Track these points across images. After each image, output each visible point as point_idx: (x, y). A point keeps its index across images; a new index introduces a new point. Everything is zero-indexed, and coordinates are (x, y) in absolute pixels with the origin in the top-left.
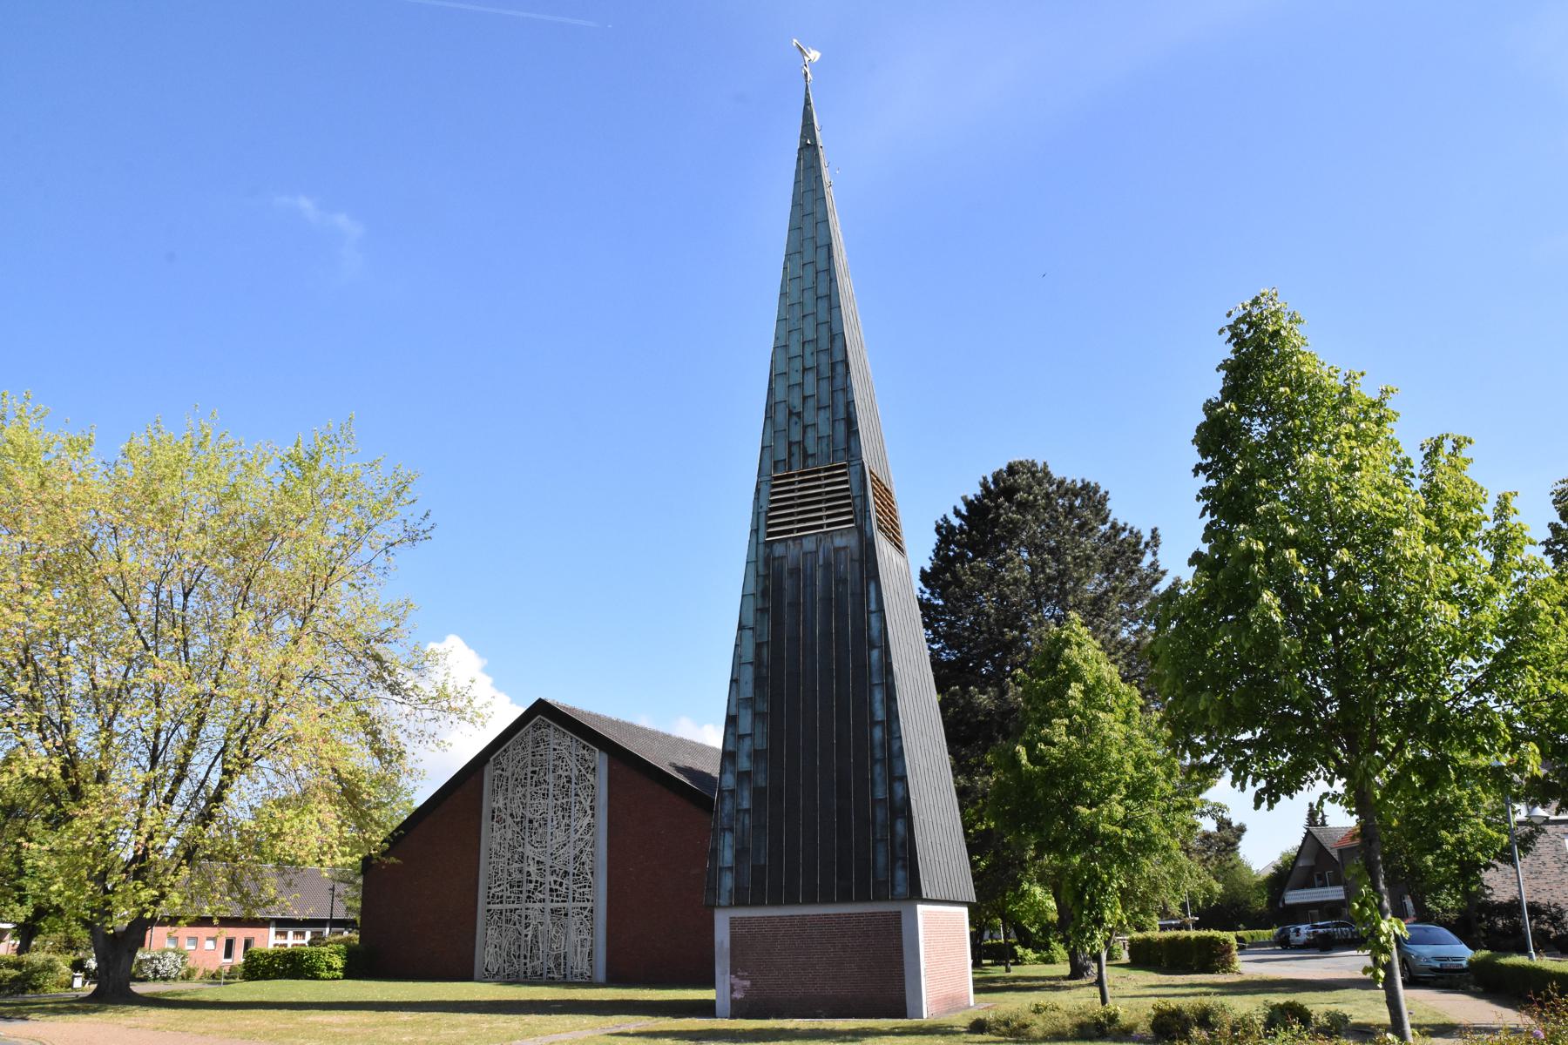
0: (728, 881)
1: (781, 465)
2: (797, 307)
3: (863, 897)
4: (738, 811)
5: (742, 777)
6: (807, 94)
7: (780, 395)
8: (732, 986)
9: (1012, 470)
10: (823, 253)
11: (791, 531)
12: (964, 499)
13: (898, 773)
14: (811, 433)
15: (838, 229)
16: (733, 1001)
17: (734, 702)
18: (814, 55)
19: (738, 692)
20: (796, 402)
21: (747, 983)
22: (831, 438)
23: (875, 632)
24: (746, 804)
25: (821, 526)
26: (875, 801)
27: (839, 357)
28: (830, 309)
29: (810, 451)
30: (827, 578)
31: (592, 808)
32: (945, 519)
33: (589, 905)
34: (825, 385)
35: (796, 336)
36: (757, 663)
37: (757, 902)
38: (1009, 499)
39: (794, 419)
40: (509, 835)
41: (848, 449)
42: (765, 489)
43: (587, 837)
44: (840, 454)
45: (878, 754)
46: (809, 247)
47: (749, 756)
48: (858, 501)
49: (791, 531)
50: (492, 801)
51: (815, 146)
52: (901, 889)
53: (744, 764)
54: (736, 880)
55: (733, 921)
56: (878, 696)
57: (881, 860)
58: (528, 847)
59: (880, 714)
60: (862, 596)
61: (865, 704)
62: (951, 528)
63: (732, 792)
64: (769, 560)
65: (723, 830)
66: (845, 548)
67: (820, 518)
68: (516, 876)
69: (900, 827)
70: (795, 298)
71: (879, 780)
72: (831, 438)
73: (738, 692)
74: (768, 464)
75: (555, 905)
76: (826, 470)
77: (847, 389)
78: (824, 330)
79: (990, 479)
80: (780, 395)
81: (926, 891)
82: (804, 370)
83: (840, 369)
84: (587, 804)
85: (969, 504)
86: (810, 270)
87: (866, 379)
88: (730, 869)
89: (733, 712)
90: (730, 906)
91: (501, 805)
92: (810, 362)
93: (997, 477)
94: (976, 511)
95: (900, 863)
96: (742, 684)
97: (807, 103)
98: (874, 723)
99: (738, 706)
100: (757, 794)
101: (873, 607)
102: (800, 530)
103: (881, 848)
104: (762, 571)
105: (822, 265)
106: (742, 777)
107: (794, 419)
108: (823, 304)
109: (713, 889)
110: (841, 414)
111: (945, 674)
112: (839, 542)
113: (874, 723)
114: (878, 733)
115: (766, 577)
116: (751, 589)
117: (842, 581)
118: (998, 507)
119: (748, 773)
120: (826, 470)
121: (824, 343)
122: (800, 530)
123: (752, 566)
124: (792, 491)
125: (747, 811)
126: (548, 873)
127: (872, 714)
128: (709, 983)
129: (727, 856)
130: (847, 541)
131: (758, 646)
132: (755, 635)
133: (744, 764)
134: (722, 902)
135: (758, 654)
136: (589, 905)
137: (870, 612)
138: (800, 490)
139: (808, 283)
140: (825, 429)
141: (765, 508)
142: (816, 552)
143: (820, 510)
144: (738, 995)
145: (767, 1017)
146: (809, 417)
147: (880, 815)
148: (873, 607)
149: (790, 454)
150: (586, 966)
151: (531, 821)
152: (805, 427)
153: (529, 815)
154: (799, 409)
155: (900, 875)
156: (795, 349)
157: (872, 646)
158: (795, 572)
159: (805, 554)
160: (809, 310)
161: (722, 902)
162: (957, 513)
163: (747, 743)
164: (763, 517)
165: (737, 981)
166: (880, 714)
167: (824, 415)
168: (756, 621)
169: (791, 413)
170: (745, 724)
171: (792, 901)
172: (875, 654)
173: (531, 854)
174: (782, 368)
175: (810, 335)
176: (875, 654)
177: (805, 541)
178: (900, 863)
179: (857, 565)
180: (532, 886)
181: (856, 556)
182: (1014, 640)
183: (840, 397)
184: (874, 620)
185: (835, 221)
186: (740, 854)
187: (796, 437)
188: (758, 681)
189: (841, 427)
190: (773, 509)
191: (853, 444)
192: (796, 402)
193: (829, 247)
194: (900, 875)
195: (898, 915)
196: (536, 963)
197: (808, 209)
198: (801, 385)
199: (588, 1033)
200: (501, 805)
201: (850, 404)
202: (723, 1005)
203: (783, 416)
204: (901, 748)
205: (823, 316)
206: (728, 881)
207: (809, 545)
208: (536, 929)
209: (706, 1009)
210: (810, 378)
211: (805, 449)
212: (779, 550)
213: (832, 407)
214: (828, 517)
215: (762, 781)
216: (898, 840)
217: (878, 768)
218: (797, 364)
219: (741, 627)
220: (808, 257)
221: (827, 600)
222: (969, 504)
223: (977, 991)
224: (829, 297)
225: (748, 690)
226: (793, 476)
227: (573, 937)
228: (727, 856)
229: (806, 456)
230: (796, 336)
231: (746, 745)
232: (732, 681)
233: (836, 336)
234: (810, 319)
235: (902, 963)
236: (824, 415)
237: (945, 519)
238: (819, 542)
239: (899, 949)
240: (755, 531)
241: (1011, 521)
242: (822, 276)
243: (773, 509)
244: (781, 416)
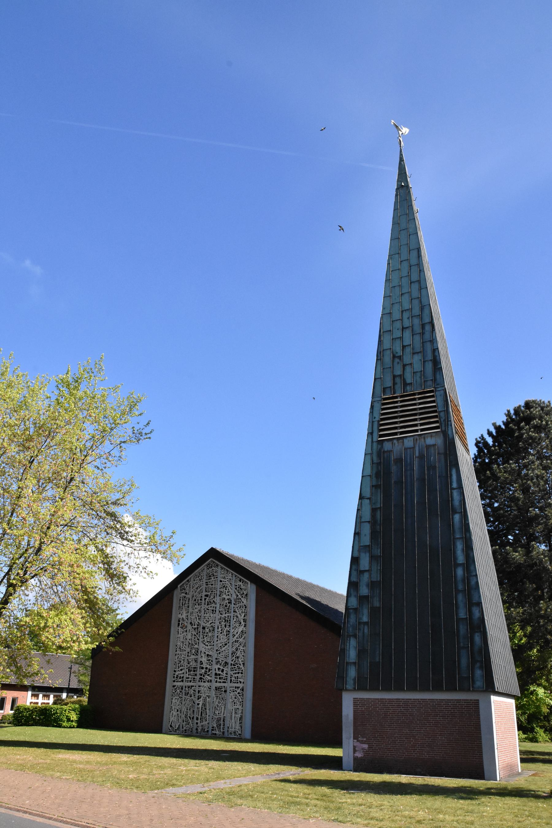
0: (352, 672)
1: (388, 391)
2: (397, 289)
3: (451, 688)
4: (360, 623)
5: (362, 599)
6: (401, 155)
7: (387, 344)
8: (354, 747)
9: (528, 405)
10: (414, 254)
11: (396, 434)
12: (494, 424)
13: (475, 600)
14: (408, 369)
15: (423, 240)
16: (355, 759)
17: (356, 548)
18: (405, 130)
19: (359, 541)
20: (398, 349)
21: (366, 746)
22: (423, 373)
23: (456, 503)
24: (365, 619)
25: (416, 431)
26: (459, 620)
27: (427, 320)
28: (420, 289)
29: (408, 381)
30: (421, 467)
31: (245, 621)
32: (482, 437)
33: (241, 685)
34: (417, 338)
35: (397, 307)
36: (373, 522)
37: (374, 688)
38: (528, 423)
39: (397, 360)
40: (189, 637)
41: (434, 380)
42: (377, 406)
43: (241, 640)
44: (430, 383)
45: (460, 587)
46: (404, 250)
47: (368, 585)
48: (442, 414)
49: (396, 434)
50: (179, 614)
51: (407, 187)
52: (479, 683)
53: (364, 591)
54: (359, 671)
55: (356, 701)
56: (459, 546)
57: (464, 662)
58: (202, 645)
59: (461, 559)
60: (447, 478)
61: (450, 552)
62: (486, 444)
63: (356, 610)
64: (381, 453)
65: (349, 636)
66: (434, 445)
67: (416, 425)
68: (193, 664)
69: (477, 638)
70: (396, 282)
71: (461, 605)
72: (423, 373)
73: (359, 541)
74: (379, 389)
75: (218, 685)
76: (420, 393)
77: (433, 341)
78: (416, 302)
79: (512, 412)
80: (387, 344)
81: (498, 686)
82: (403, 328)
83: (428, 328)
84: (241, 618)
85: (498, 428)
86: (405, 265)
87: (442, 336)
88: (354, 663)
89: (356, 555)
90: (354, 690)
91: (184, 616)
92: (407, 323)
93: (517, 411)
94: (501, 434)
95: (478, 665)
96: (362, 536)
97: (401, 160)
98: (457, 565)
99: (359, 551)
100: (373, 612)
101: (455, 485)
102: (402, 433)
103: (464, 653)
104: (375, 459)
105: (414, 261)
106: (362, 599)
107: (397, 360)
108: (415, 286)
109: (342, 677)
110: (430, 356)
111: (494, 536)
112: (430, 441)
113: (457, 565)
114: (460, 572)
115: (379, 464)
116: (368, 472)
117: (432, 468)
118: (520, 429)
119: (366, 598)
120: (420, 393)
121: (416, 311)
122: (402, 433)
123: (369, 457)
124: (396, 407)
125: (366, 623)
126: (214, 663)
127: (455, 559)
128: (337, 743)
129: (352, 655)
130: (435, 440)
131: (374, 511)
132: (371, 503)
133: (364, 591)
134: (348, 687)
135: (373, 516)
136: (241, 685)
137: (452, 489)
138: (402, 406)
139: (405, 273)
140: (418, 367)
141: (377, 419)
142: (414, 448)
143: (415, 420)
144: (359, 755)
145: (381, 772)
146: (407, 359)
147: (463, 630)
148: (455, 485)
149: (394, 384)
150: (238, 727)
151: (204, 628)
152: (404, 366)
153: (203, 624)
154: (400, 353)
155: (478, 673)
156: (397, 315)
157: (454, 512)
158: (399, 461)
159: (406, 449)
160: (405, 290)
161: (348, 687)
162: (490, 434)
163: (366, 575)
164: (376, 424)
165: (357, 744)
166: (461, 559)
167: (417, 358)
168: (372, 494)
169: (394, 357)
170: (365, 563)
171: (399, 688)
172: (457, 517)
173: (203, 650)
174: (387, 327)
175: (406, 306)
176: (457, 517)
177: (406, 441)
178: (478, 665)
179: (442, 457)
180: (203, 671)
181: (442, 451)
182: (537, 516)
183: (428, 346)
184: (455, 494)
185: (421, 234)
186: (361, 653)
187: (398, 372)
188: (374, 534)
189: (429, 366)
190: (382, 419)
191: (438, 376)
192: (398, 349)
193: (419, 250)
194: (478, 673)
195: (477, 702)
196: (205, 723)
197: (403, 226)
198: (401, 338)
199: (260, 780)
200: (184, 616)
201: (435, 350)
202: (348, 761)
203: (389, 359)
204: (477, 583)
205: (415, 294)
206: (352, 672)
207: (409, 443)
208: (205, 700)
209: (335, 763)
210: (407, 334)
211: (404, 380)
212: (387, 446)
213: (423, 352)
214: (422, 424)
215: (377, 604)
216: (476, 648)
217: (460, 597)
218: (398, 325)
219: (361, 498)
220: (404, 256)
221: (422, 480)
222: (498, 428)
223: (523, 760)
224: (419, 281)
225: (366, 540)
226: (396, 397)
227: (230, 706)
228: (352, 655)
229: (405, 384)
230: (397, 307)
231: (366, 577)
232: (355, 534)
233: (424, 307)
234: (406, 297)
235: (480, 738)
236: (417, 358)
237: (482, 437)
238: (415, 441)
239: (478, 727)
240: (370, 434)
241: (531, 438)
242: (415, 269)
243: (382, 419)
244: (388, 358)
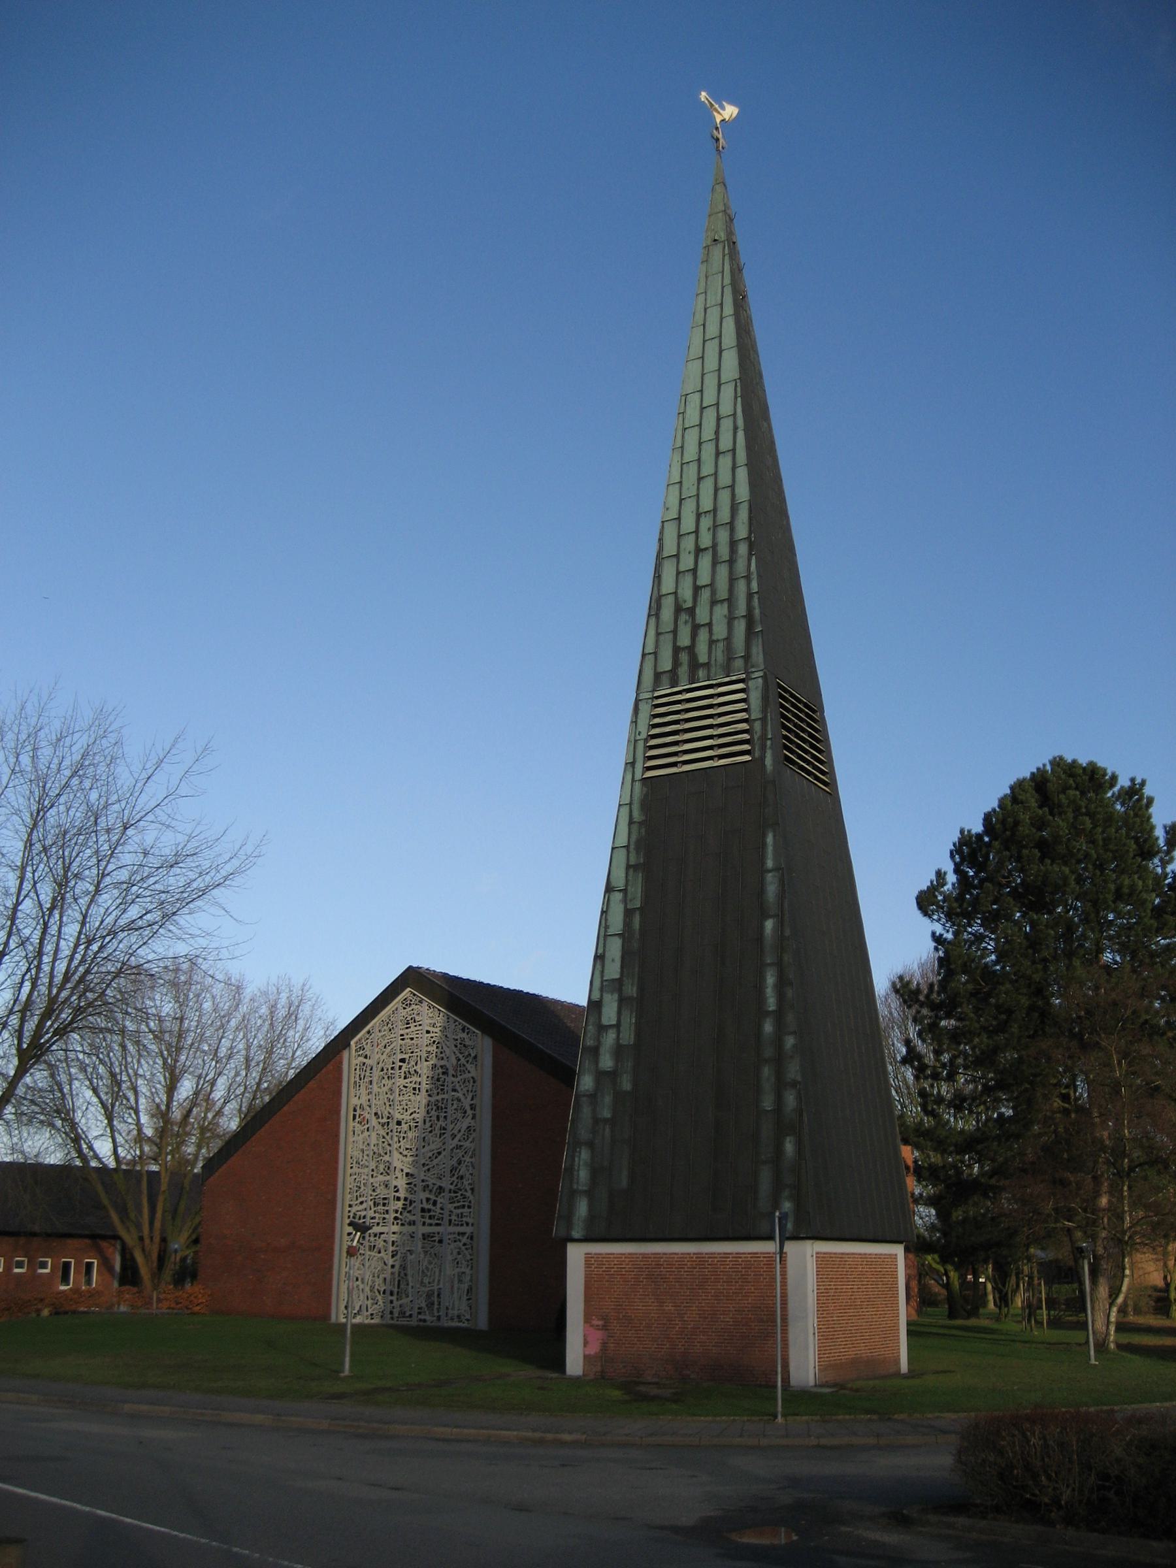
0: (582, 1208)
1: (665, 679)
14: (703, 635)
17: (597, 983)
24: (606, 1114)
29: (703, 658)
31: (473, 1107)
33: (468, 1230)
39: (684, 617)
40: (373, 1141)
43: (467, 1144)
48: (757, 726)
50: (353, 1097)
58: (396, 1155)
68: (382, 1192)
75: (427, 1230)
84: (467, 1103)
91: (364, 1100)
95: (786, 1193)
96: (607, 962)
99: (602, 990)
114: (768, 1027)
116: (623, 840)
123: (625, 810)
125: (606, 1120)
126: (419, 1189)
131: (628, 913)
132: (625, 901)
135: (627, 923)
136: (468, 1230)
140: (720, 631)
141: (644, 736)
146: (702, 615)
149: (676, 663)
150: (464, 1307)
151: (399, 1123)
153: (398, 1116)
161: (576, 1234)
164: (641, 745)
167: (721, 611)
173: (399, 1165)
180: (400, 1204)
186: (596, 1172)
192: (687, 593)
196: (404, 1301)
198: (694, 571)
200: (364, 1100)
206: (582, 1208)
208: (404, 1259)
210: (705, 562)
217: (766, 1071)
219: (609, 889)
225: (613, 970)
227: (449, 1270)
229: (694, 665)
244: (667, 613)
